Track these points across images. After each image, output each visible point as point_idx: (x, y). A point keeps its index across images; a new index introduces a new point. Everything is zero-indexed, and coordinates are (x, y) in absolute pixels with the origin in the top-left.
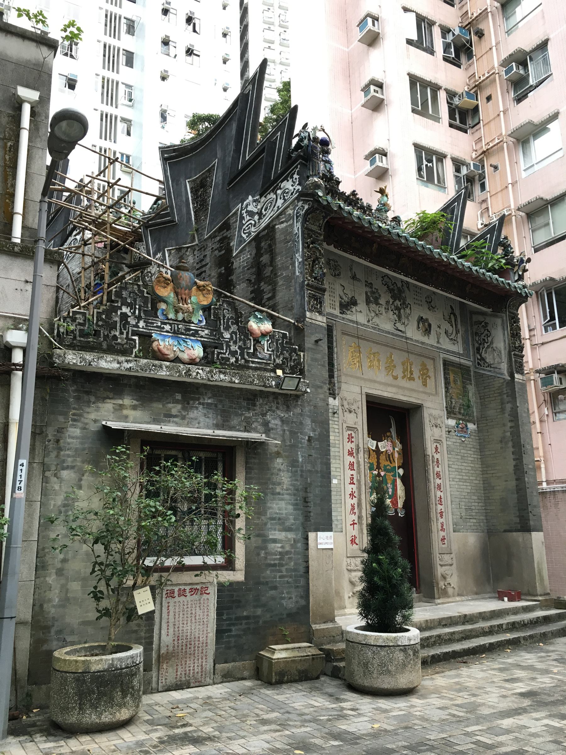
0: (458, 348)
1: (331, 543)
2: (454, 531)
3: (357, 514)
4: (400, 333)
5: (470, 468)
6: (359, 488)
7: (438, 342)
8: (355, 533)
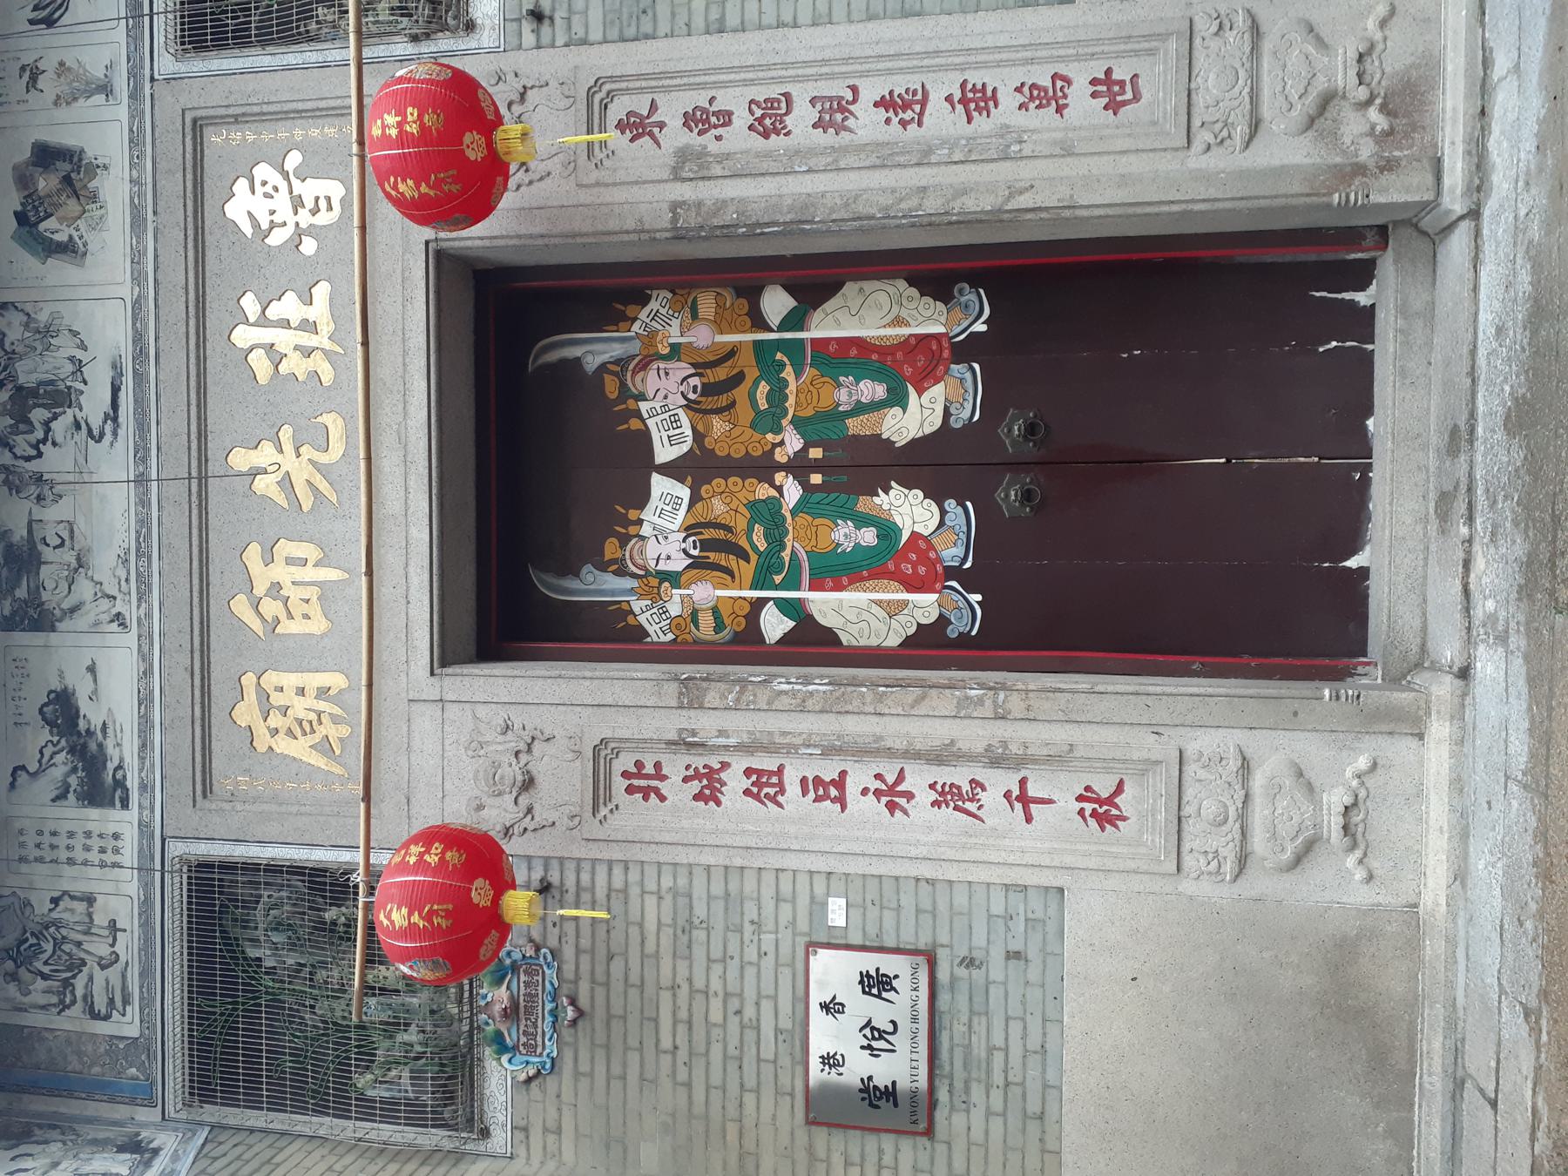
3: (981, 774)
4: (128, 382)
6: (862, 752)
7: (106, 89)
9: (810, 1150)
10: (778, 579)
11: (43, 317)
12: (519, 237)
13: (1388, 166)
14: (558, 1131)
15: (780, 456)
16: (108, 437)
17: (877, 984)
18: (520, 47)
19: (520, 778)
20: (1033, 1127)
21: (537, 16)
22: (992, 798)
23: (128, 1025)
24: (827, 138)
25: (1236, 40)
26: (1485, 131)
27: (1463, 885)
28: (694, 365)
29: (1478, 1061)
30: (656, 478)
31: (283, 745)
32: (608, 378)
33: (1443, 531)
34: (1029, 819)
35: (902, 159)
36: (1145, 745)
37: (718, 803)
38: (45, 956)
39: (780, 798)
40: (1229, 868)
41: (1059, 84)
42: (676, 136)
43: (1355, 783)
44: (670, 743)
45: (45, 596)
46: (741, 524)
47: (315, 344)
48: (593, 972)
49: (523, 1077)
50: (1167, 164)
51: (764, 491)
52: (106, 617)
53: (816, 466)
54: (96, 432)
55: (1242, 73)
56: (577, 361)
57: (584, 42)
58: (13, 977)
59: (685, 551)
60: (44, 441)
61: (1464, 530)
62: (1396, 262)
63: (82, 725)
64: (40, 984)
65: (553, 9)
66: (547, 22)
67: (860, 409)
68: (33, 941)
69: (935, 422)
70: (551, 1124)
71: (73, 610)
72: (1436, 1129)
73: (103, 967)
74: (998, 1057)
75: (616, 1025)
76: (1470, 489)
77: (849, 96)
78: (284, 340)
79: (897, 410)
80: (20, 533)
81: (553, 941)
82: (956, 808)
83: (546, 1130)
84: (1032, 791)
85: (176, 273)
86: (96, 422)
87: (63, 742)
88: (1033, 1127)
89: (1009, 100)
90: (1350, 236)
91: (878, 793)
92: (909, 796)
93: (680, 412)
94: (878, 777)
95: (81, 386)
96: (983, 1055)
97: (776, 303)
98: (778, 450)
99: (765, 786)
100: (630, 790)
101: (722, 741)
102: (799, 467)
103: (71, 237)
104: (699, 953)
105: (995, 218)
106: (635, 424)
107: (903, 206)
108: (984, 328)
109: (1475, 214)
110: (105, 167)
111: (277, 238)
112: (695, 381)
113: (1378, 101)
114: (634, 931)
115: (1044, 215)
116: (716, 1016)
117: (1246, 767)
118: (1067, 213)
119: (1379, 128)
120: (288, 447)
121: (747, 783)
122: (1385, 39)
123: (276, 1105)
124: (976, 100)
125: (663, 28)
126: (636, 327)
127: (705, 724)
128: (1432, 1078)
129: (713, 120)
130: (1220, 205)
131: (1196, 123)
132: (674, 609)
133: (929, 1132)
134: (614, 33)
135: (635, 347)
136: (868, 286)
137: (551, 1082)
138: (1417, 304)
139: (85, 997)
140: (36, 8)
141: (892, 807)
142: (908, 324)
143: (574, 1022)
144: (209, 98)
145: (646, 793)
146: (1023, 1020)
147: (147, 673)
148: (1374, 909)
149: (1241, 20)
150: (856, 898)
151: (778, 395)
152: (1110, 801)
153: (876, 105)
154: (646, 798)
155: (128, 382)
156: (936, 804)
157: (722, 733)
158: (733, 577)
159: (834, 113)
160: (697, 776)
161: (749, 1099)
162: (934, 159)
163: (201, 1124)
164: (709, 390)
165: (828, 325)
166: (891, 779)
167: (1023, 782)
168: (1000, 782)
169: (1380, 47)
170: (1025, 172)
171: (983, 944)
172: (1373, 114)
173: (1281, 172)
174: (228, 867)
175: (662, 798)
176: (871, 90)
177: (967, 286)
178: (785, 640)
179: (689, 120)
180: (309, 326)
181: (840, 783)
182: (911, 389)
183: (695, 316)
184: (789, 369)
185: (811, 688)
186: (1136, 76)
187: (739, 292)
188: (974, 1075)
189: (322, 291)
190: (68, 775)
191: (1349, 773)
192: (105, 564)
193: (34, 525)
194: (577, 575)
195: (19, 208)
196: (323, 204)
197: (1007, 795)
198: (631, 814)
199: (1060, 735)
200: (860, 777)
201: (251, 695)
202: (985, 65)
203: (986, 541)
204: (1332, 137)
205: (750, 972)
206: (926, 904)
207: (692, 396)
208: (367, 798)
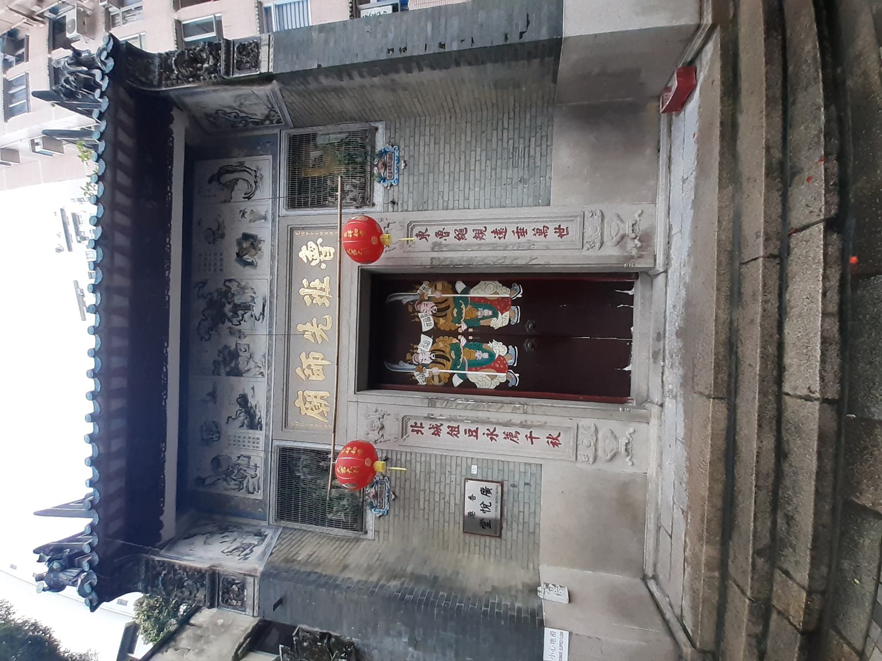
0: (264, 164)
1: (562, 634)
2: (549, 204)
4: (268, 303)
5: (447, 147)
6: (483, 422)
7: (265, 218)
8: (542, 435)
9: (464, 540)
10: (458, 367)
11: (243, 284)
12: (385, 266)
13: (640, 257)
14: (388, 533)
15: (460, 331)
16: (261, 320)
17: (486, 492)
18: (388, 211)
19: (380, 426)
20: (531, 536)
21: (393, 203)
22: (521, 437)
23: (259, 496)
24: (478, 241)
25: (597, 219)
26: (669, 248)
27: (661, 468)
28: (435, 303)
29: (666, 523)
30: (422, 335)
31: (310, 413)
32: (409, 306)
33: (654, 362)
34: (532, 443)
35: (499, 248)
36: (567, 423)
37: (439, 436)
38: (235, 474)
39: (458, 435)
40: (591, 460)
41: (545, 229)
42: (433, 238)
43: (629, 436)
44: (425, 417)
45: (240, 366)
46: (448, 350)
47: (323, 295)
48: (400, 484)
49: (378, 515)
50: (576, 253)
51: (455, 341)
52: (258, 373)
53: (471, 334)
54: (258, 318)
55: (598, 228)
56: (401, 301)
57: (407, 211)
58: (225, 480)
59: (430, 358)
60: (242, 320)
61: (662, 363)
62: (641, 283)
63: (249, 405)
64: (233, 482)
65: (398, 201)
66: (396, 204)
67: (484, 318)
68: (231, 469)
69: (506, 323)
70: (386, 529)
71: (248, 370)
72: (652, 539)
73: (252, 478)
74: (522, 514)
75: (407, 501)
76: (664, 351)
77: (484, 230)
78: (315, 293)
79: (495, 319)
80: (233, 347)
81: (388, 475)
82: (511, 440)
83: (385, 532)
84: (533, 436)
85: (284, 272)
86: (258, 315)
87: (243, 410)
88: (531, 536)
89: (530, 233)
90: (628, 275)
91: (488, 435)
92: (497, 436)
93: (431, 317)
94: (488, 430)
95: (254, 304)
96: (517, 513)
97: (460, 286)
98: (459, 329)
99: (453, 431)
100: (413, 431)
101: (441, 418)
102: (466, 334)
103: (253, 261)
104: (432, 480)
105: (527, 266)
106: (417, 320)
107: (499, 261)
108: (521, 296)
109: (666, 272)
110: (264, 241)
111: (314, 263)
112: (435, 308)
113: (638, 238)
114: (413, 473)
115: (540, 266)
116: (437, 499)
117: (596, 430)
118: (547, 266)
119: (638, 246)
120: (315, 324)
121: (448, 430)
122: (640, 220)
123: (303, 522)
124: (521, 232)
125: (430, 208)
126: (418, 291)
127: (436, 412)
128: (651, 525)
129: (444, 235)
130: (591, 266)
131: (585, 242)
132: (427, 375)
133: (500, 536)
134: (415, 209)
135: (418, 297)
136: (487, 282)
137: (386, 517)
138: (647, 295)
139: (246, 487)
140: (245, 194)
141: (492, 439)
142: (499, 294)
143: (394, 500)
144: (296, 222)
145: (418, 432)
146: (529, 503)
147: (269, 390)
148: (634, 474)
149: (598, 213)
150: (480, 465)
151: (460, 313)
152: (556, 439)
153: (492, 232)
154: (417, 433)
155: (268, 303)
156: (505, 438)
157: (441, 415)
158: (444, 366)
159: (479, 234)
160: (433, 427)
161: (446, 524)
162: (508, 249)
163: (280, 527)
164: (439, 310)
165: (475, 293)
166: (492, 431)
167: (531, 432)
168: (525, 432)
169: (639, 222)
170: (535, 254)
171: (518, 480)
172: (636, 241)
173: (610, 256)
174: (291, 449)
175: (422, 434)
176: (491, 228)
177: (516, 284)
178: (460, 385)
179: (437, 234)
180: (322, 289)
181: (476, 432)
182: (499, 312)
183: (436, 288)
184: (463, 305)
185: (468, 402)
186: (567, 227)
187: (449, 282)
188: (514, 519)
189: (327, 279)
190: (245, 419)
191: (627, 433)
192: (258, 358)
193: (238, 345)
194: (398, 364)
195: (237, 252)
196: (328, 254)
197: (526, 436)
198: (413, 438)
199: (542, 419)
200: (482, 429)
201: (301, 397)
202: (524, 222)
203: (520, 358)
204: (624, 248)
205: (448, 487)
206: (501, 468)
207: (434, 312)
208: (334, 432)
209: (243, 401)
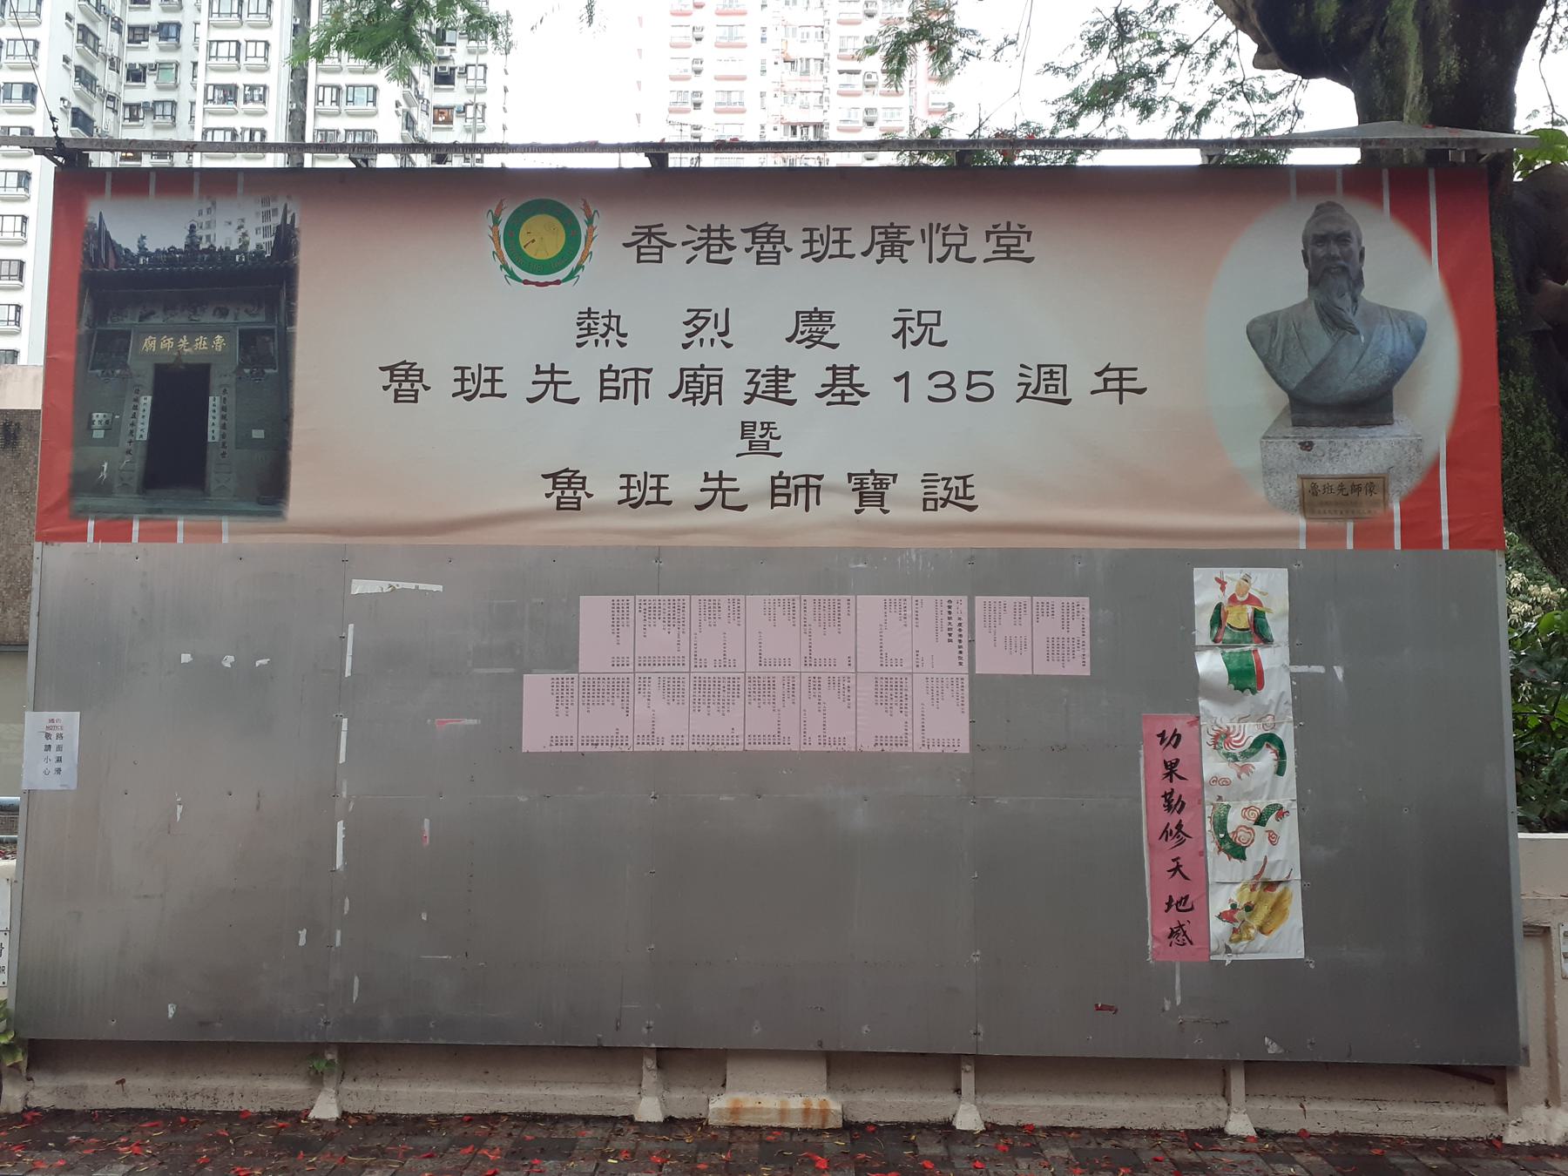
0: (261, 318)
7: (236, 319)
23: (109, 322)
78: (200, 343)
192: (172, 319)
209: (153, 313)
